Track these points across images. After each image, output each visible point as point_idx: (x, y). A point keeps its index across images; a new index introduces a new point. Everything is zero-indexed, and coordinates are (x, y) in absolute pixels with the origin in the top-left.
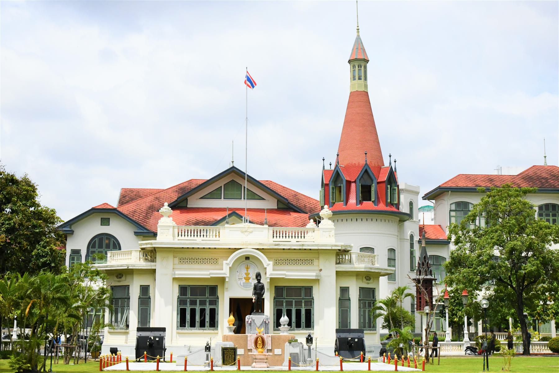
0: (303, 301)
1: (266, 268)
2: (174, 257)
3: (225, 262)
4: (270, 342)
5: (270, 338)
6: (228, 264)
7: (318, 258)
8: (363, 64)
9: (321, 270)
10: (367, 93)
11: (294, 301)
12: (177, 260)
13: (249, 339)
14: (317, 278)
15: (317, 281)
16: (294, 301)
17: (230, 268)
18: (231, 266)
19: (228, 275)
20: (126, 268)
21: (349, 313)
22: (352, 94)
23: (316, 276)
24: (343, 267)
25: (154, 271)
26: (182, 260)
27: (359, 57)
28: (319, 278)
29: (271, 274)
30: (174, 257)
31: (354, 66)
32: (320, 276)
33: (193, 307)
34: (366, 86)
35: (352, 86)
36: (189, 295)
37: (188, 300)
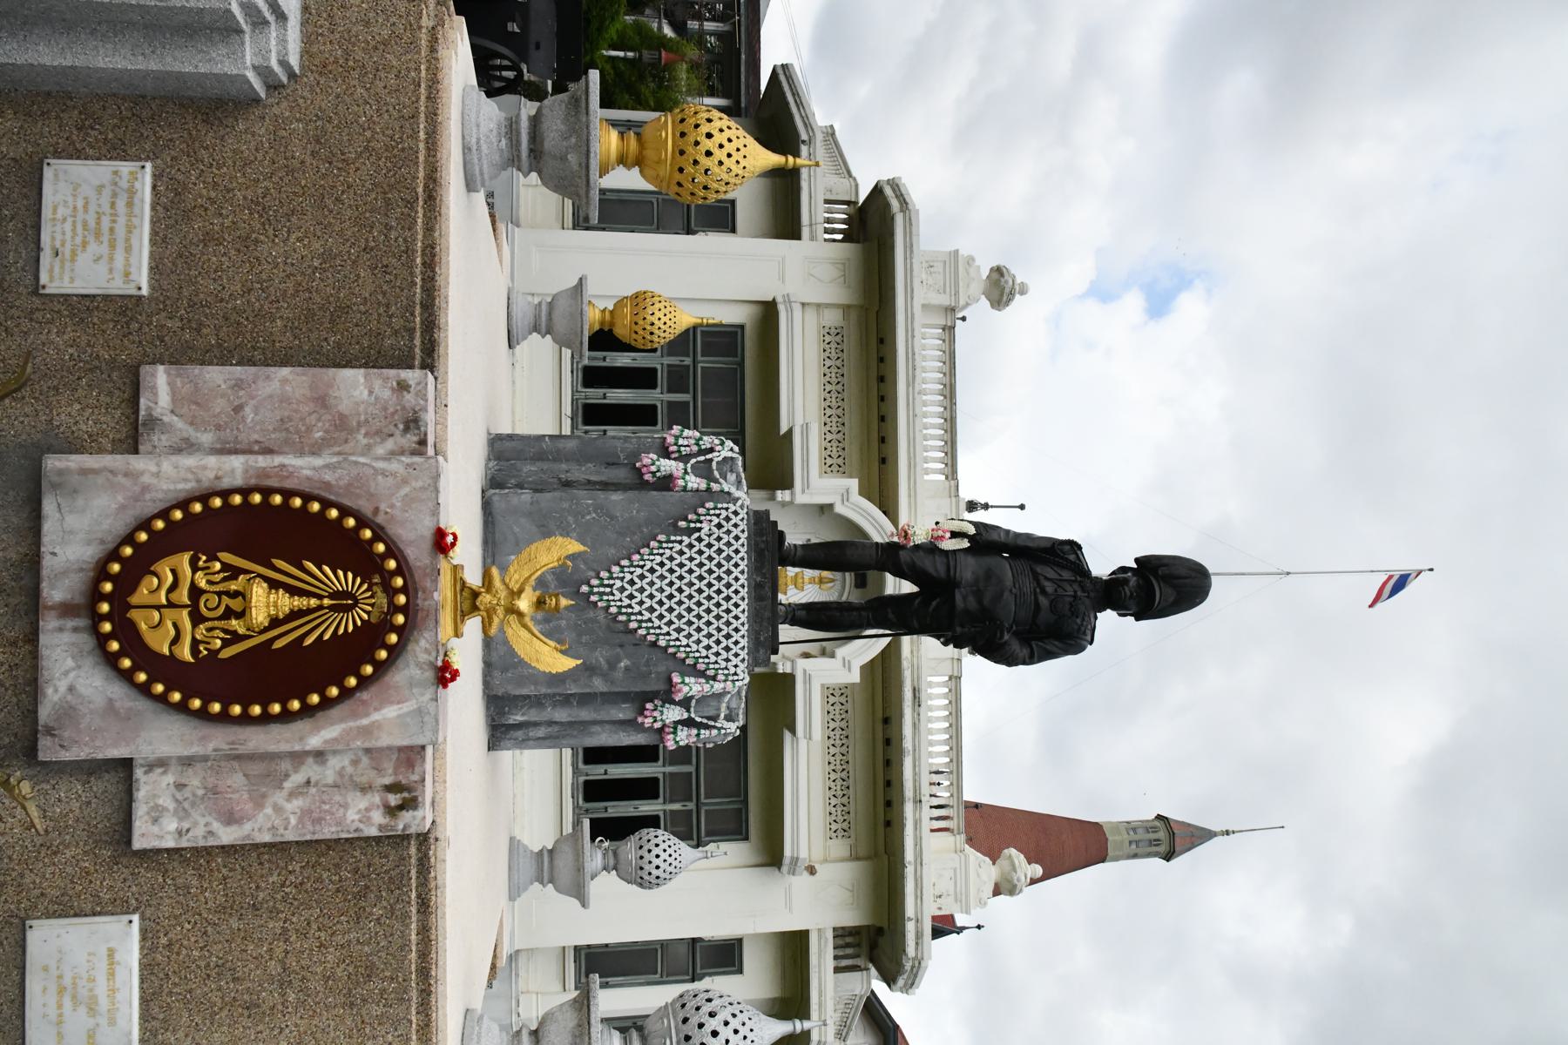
0: (691, 806)
1: (833, 656)
2: (846, 309)
3: (854, 484)
4: (277, 817)
5: (361, 814)
6: (846, 496)
7: (854, 857)
8: (1163, 849)
9: (812, 871)
10: (1103, 861)
11: (691, 769)
12: (833, 318)
13: (355, 387)
14: (786, 861)
15: (772, 856)
16: (691, 769)
17: (831, 506)
18: (839, 509)
19: (801, 498)
20: (804, 136)
21: (642, 978)
22: (1097, 826)
23: (795, 861)
24: (822, 958)
25: (796, 235)
26: (833, 339)
27: (1177, 840)
28: (785, 868)
29: (808, 679)
30: (846, 309)
31: (1155, 830)
32: (793, 872)
33: (661, 377)
34: (1116, 859)
35: (1116, 826)
36: (704, 362)
37: (688, 361)
